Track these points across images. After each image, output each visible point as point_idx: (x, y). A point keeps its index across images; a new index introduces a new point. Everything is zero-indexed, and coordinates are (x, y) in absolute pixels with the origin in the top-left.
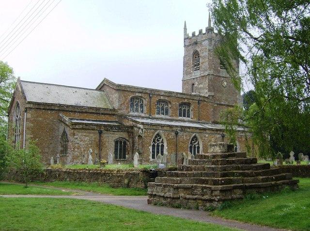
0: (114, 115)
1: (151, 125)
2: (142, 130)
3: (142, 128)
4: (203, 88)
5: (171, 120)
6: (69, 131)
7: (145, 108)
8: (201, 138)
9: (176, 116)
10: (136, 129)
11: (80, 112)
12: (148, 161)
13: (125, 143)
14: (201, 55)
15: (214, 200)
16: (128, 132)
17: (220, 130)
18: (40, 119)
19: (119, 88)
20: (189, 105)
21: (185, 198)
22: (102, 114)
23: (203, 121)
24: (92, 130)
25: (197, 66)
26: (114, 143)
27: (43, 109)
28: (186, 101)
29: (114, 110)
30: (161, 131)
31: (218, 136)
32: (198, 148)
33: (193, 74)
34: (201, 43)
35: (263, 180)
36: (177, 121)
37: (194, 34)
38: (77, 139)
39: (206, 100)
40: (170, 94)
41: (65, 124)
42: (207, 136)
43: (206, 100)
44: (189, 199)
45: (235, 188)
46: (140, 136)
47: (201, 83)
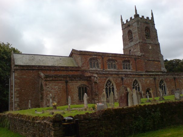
0: (78, 70)
2: (97, 78)
3: (97, 76)
4: (137, 52)
6: (44, 83)
7: (100, 65)
8: (140, 81)
9: (121, 69)
10: (92, 78)
11: (53, 70)
13: (86, 88)
14: (133, 32)
16: (87, 80)
18: (25, 76)
19: (81, 53)
20: (129, 61)
22: (70, 70)
24: (60, 80)
25: (131, 39)
26: (77, 89)
27: (27, 69)
28: (127, 59)
29: (79, 67)
30: (111, 78)
31: (151, 79)
33: (129, 44)
37: (127, 21)
38: (48, 88)
39: (140, 57)
40: (115, 55)
41: (41, 78)
42: (144, 79)
43: (140, 57)
46: (96, 83)
47: (135, 49)
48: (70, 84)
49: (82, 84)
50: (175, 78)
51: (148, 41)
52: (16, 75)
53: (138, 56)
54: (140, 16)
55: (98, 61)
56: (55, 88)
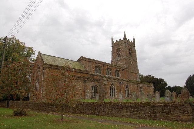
7: (101, 71)
12: (109, 97)
13: (96, 87)
20: (119, 71)
22: (83, 73)
25: (118, 55)
37: (117, 41)
46: (105, 84)
48: (87, 83)
51: (131, 58)
54: (127, 40)
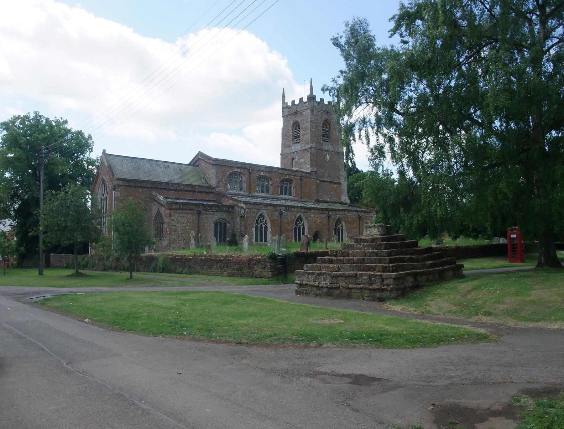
0: (211, 193)
1: (254, 204)
3: (244, 207)
5: (272, 199)
7: (244, 185)
8: (306, 218)
9: (278, 194)
10: (237, 208)
11: (173, 190)
13: (225, 225)
14: (301, 126)
15: (386, 290)
17: (327, 210)
20: (290, 181)
21: (348, 288)
22: (199, 192)
23: (306, 199)
24: (191, 210)
25: (296, 138)
26: (213, 225)
27: (134, 186)
30: (264, 211)
31: (323, 216)
32: (303, 229)
33: (293, 147)
34: (302, 113)
35: (431, 266)
36: (278, 199)
37: (293, 102)
38: (173, 220)
40: (270, 169)
42: (312, 216)
43: (308, 175)
44: (352, 289)
45: (407, 275)
47: (302, 158)
49: (221, 217)
50: (360, 218)
51: (327, 146)
52: (118, 194)
53: (306, 173)
55: (242, 178)
56: (183, 221)
